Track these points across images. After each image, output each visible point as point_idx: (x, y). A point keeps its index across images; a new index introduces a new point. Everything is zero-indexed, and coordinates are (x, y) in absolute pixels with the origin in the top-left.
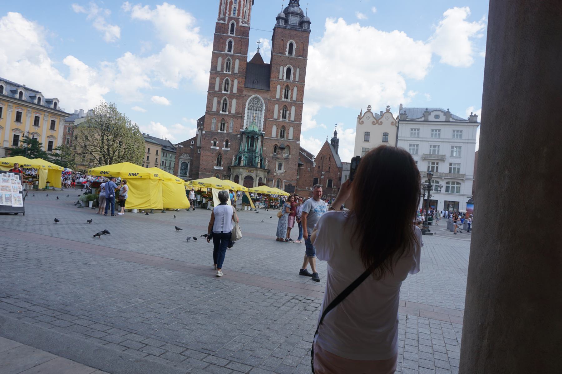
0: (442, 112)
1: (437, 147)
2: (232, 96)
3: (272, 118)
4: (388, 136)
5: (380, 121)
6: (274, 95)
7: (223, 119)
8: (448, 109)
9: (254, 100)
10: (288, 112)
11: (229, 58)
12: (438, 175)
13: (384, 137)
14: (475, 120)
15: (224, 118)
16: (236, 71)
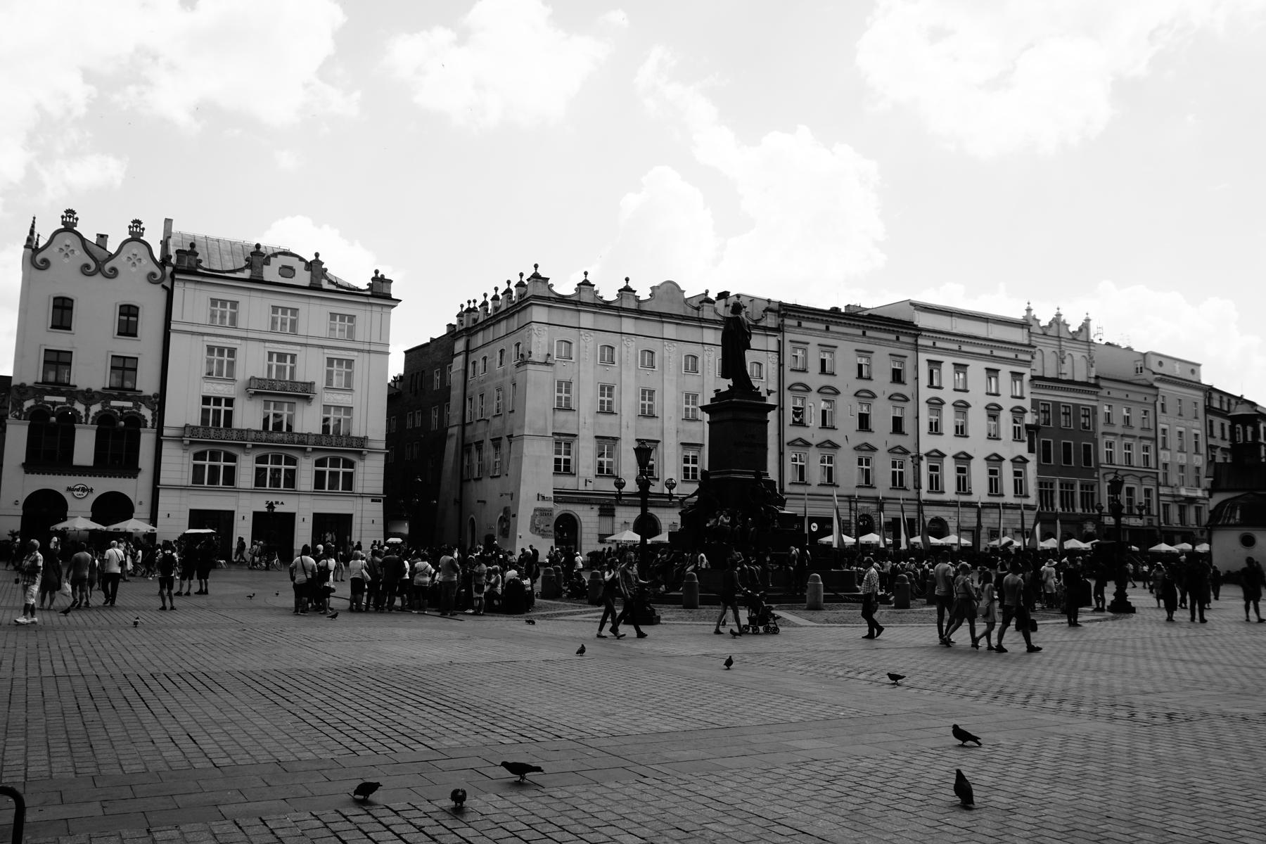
0: (301, 259)
1: (289, 358)
4: (136, 316)
5: (108, 266)
8: (317, 255)
12: (296, 440)
13: (125, 318)
14: (385, 291)
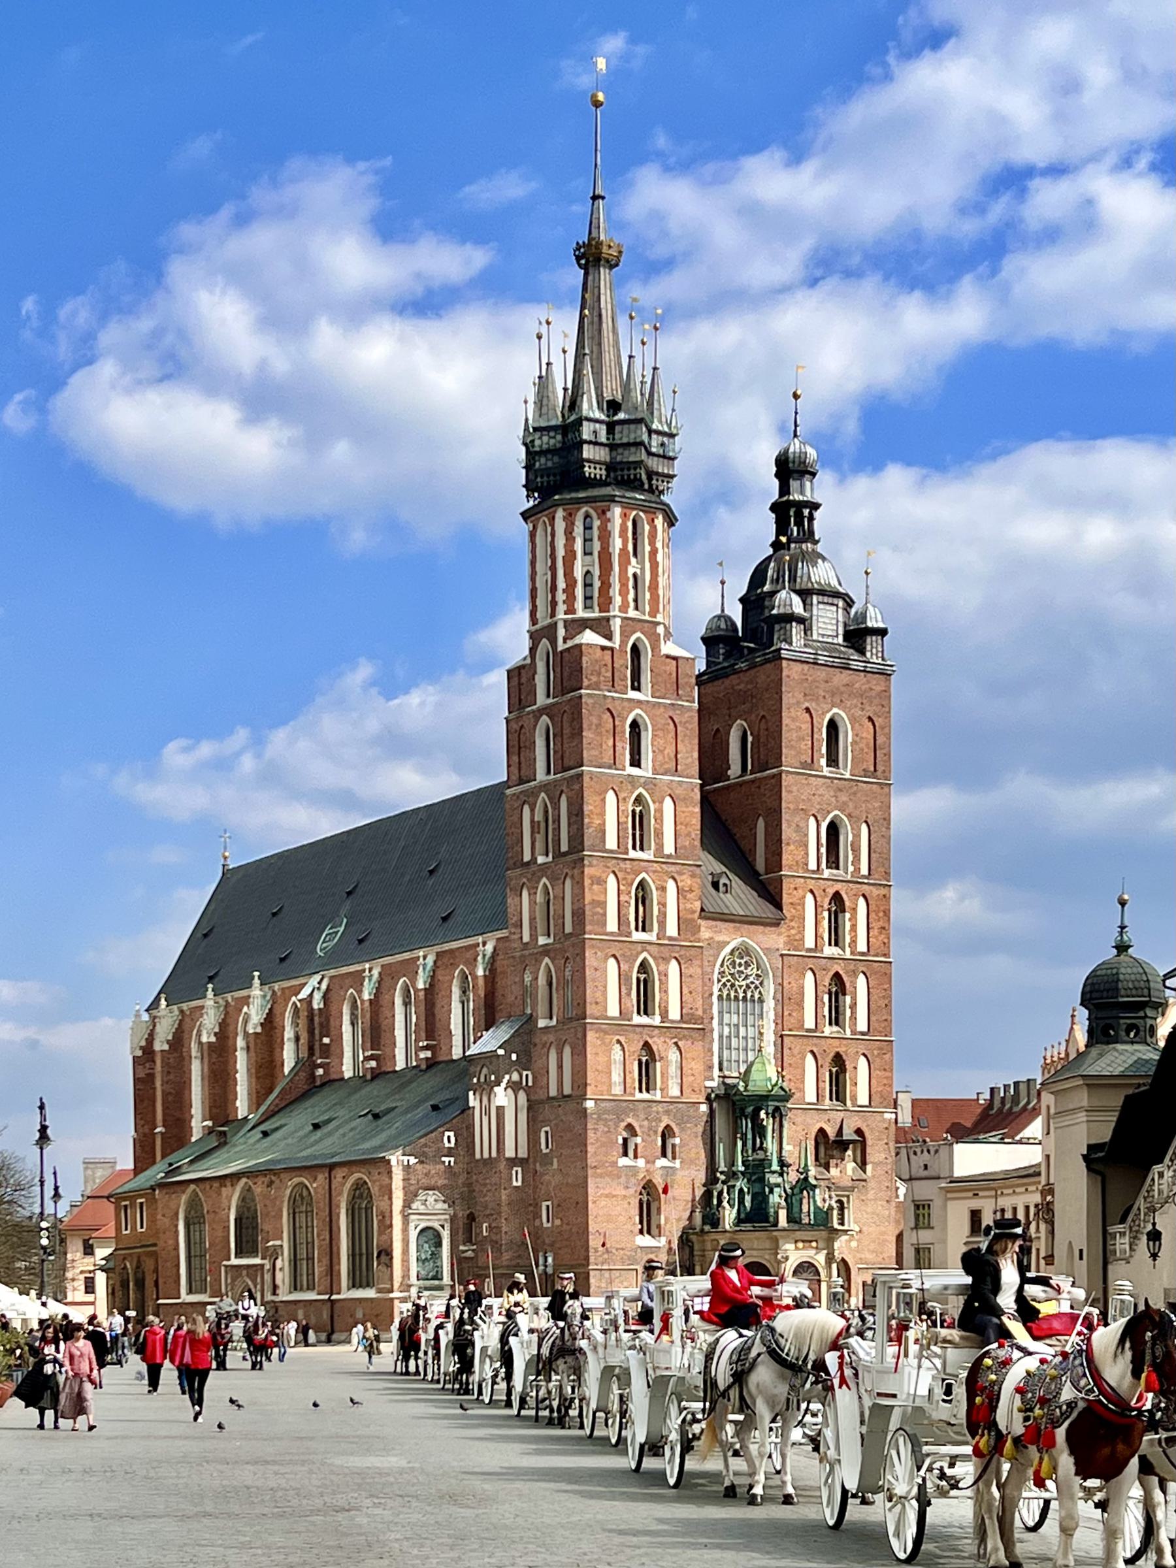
2: (668, 949)
3: (801, 1026)
6: (797, 938)
7: (647, 1046)
9: (734, 962)
10: (848, 999)
11: (639, 796)
15: (650, 1041)
16: (669, 848)
